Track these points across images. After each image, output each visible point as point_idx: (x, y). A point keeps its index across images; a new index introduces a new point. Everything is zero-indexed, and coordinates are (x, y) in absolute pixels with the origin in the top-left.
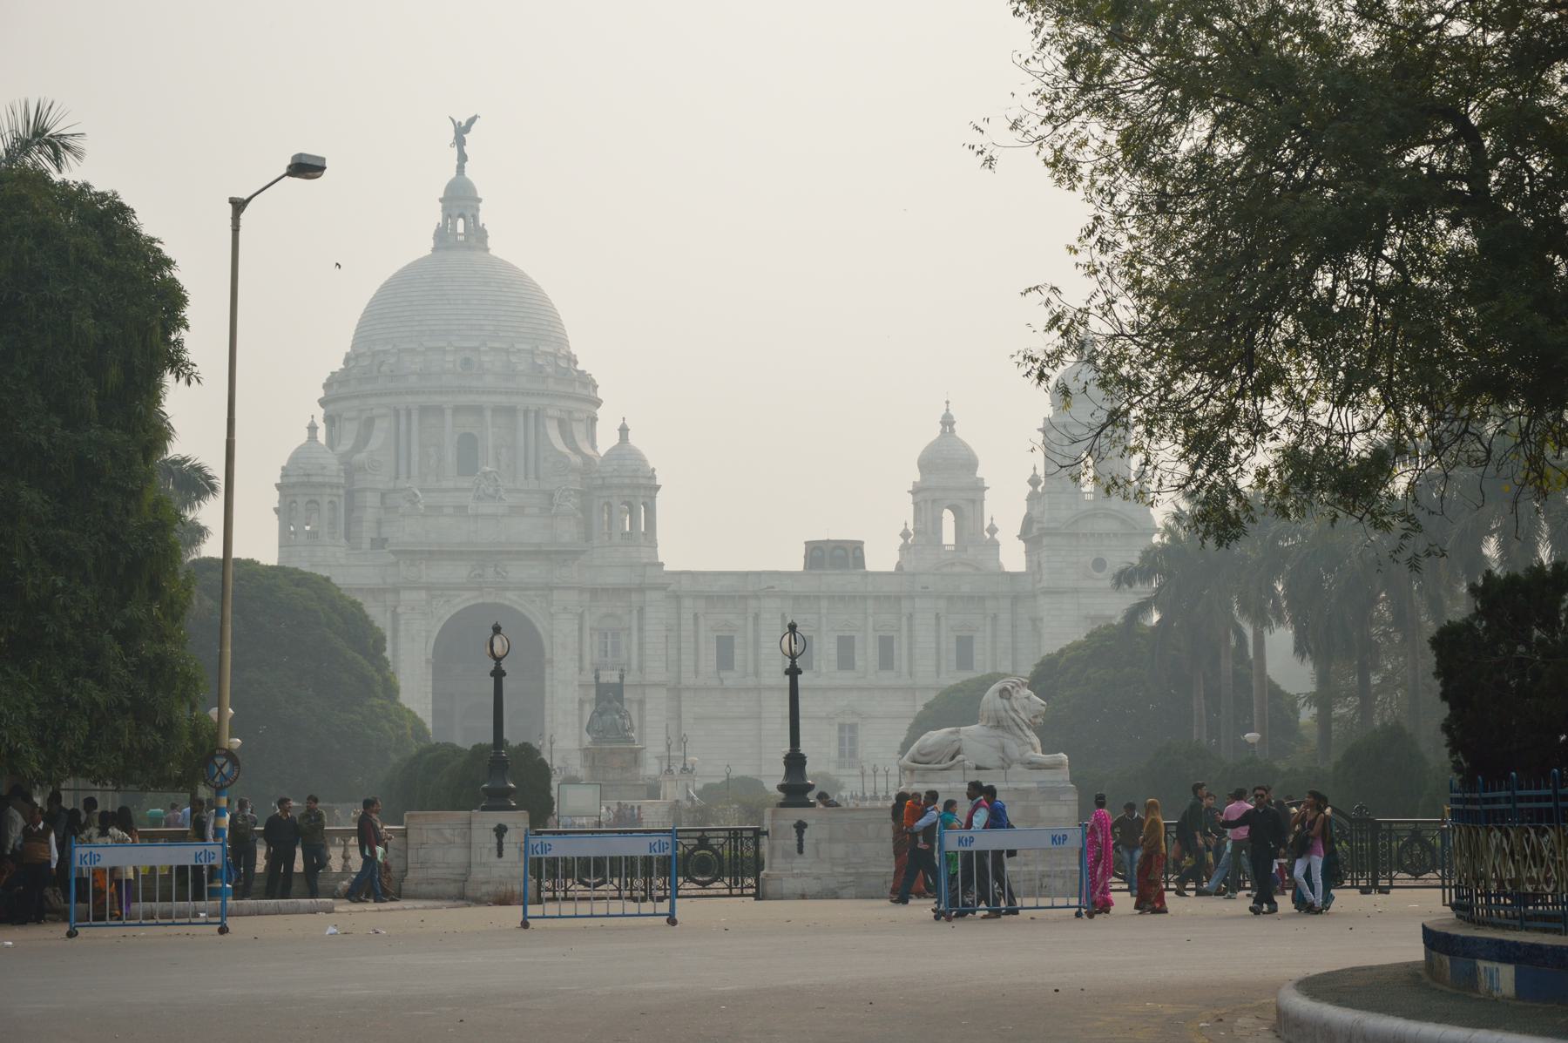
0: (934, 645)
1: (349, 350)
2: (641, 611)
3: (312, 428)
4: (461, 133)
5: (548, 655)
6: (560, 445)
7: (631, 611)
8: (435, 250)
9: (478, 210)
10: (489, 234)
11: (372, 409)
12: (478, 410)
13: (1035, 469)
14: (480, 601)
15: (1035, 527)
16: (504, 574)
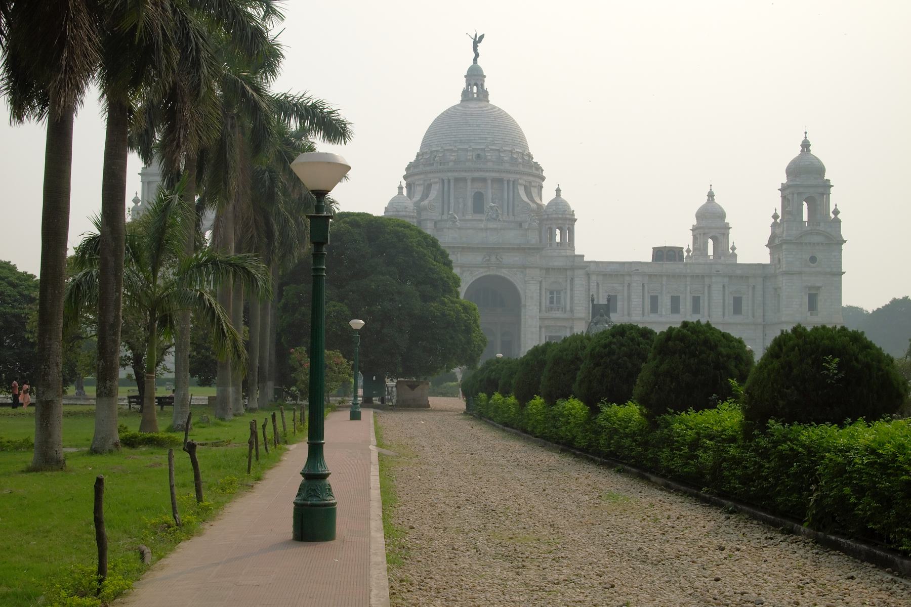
0: (722, 301)
1: (419, 151)
2: (572, 280)
3: (400, 188)
4: (477, 41)
5: (523, 303)
6: (525, 198)
7: (566, 281)
8: (462, 101)
9: (484, 81)
10: (489, 93)
11: (430, 180)
12: (484, 180)
13: (776, 210)
14: (488, 273)
15: (777, 241)
16: (501, 260)
